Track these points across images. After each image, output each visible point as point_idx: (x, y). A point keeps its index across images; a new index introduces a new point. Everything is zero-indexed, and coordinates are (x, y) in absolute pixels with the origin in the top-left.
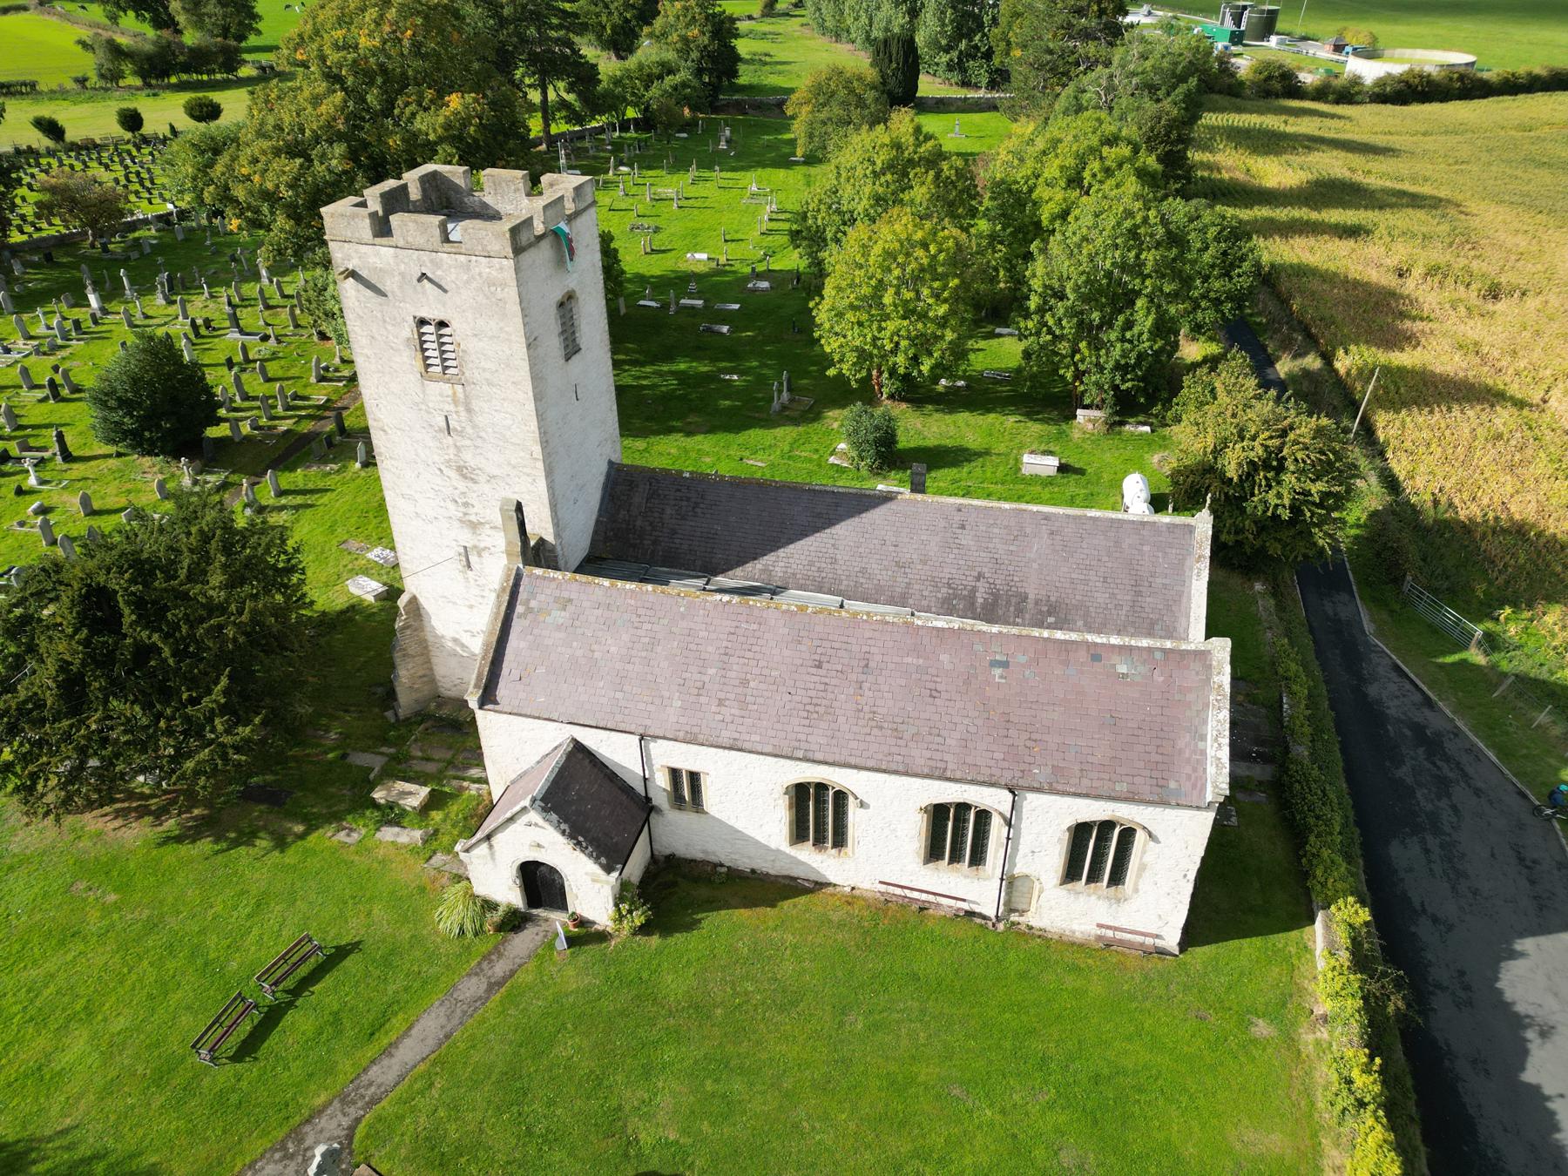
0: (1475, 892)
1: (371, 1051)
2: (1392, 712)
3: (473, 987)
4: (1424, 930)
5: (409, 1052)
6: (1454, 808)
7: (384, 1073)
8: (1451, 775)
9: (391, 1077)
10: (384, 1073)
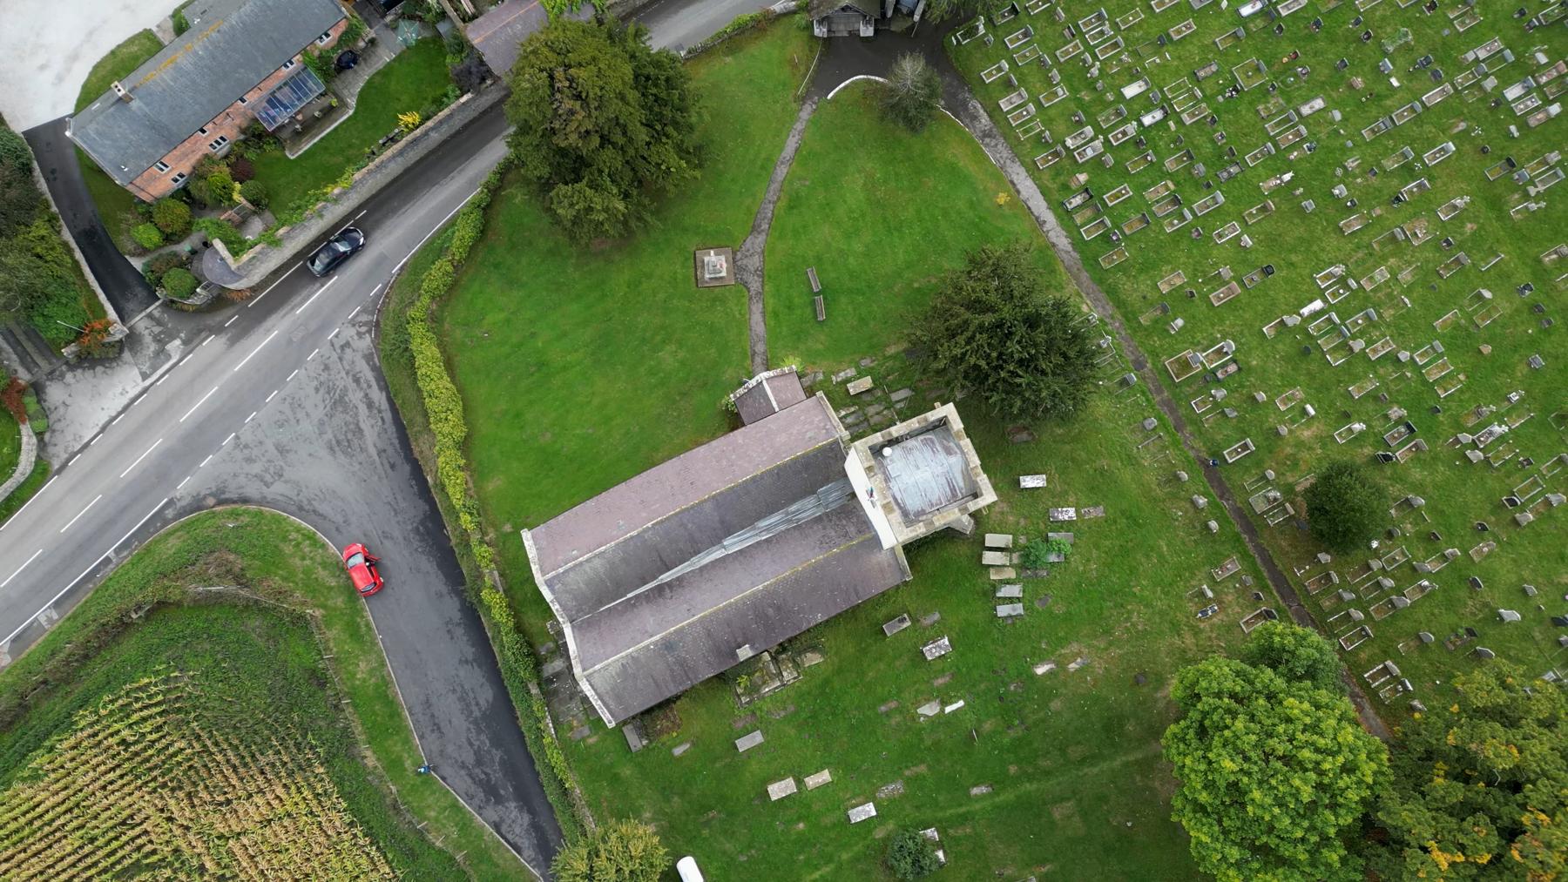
0: (454, 691)
1: (770, 309)
2: (512, 805)
3: (760, 348)
4: (470, 652)
5: (757, 317)
6: (471, 744)
7: (757, 308)
8: (477, 770)
9: (754, 308)
10: (757, 308)
